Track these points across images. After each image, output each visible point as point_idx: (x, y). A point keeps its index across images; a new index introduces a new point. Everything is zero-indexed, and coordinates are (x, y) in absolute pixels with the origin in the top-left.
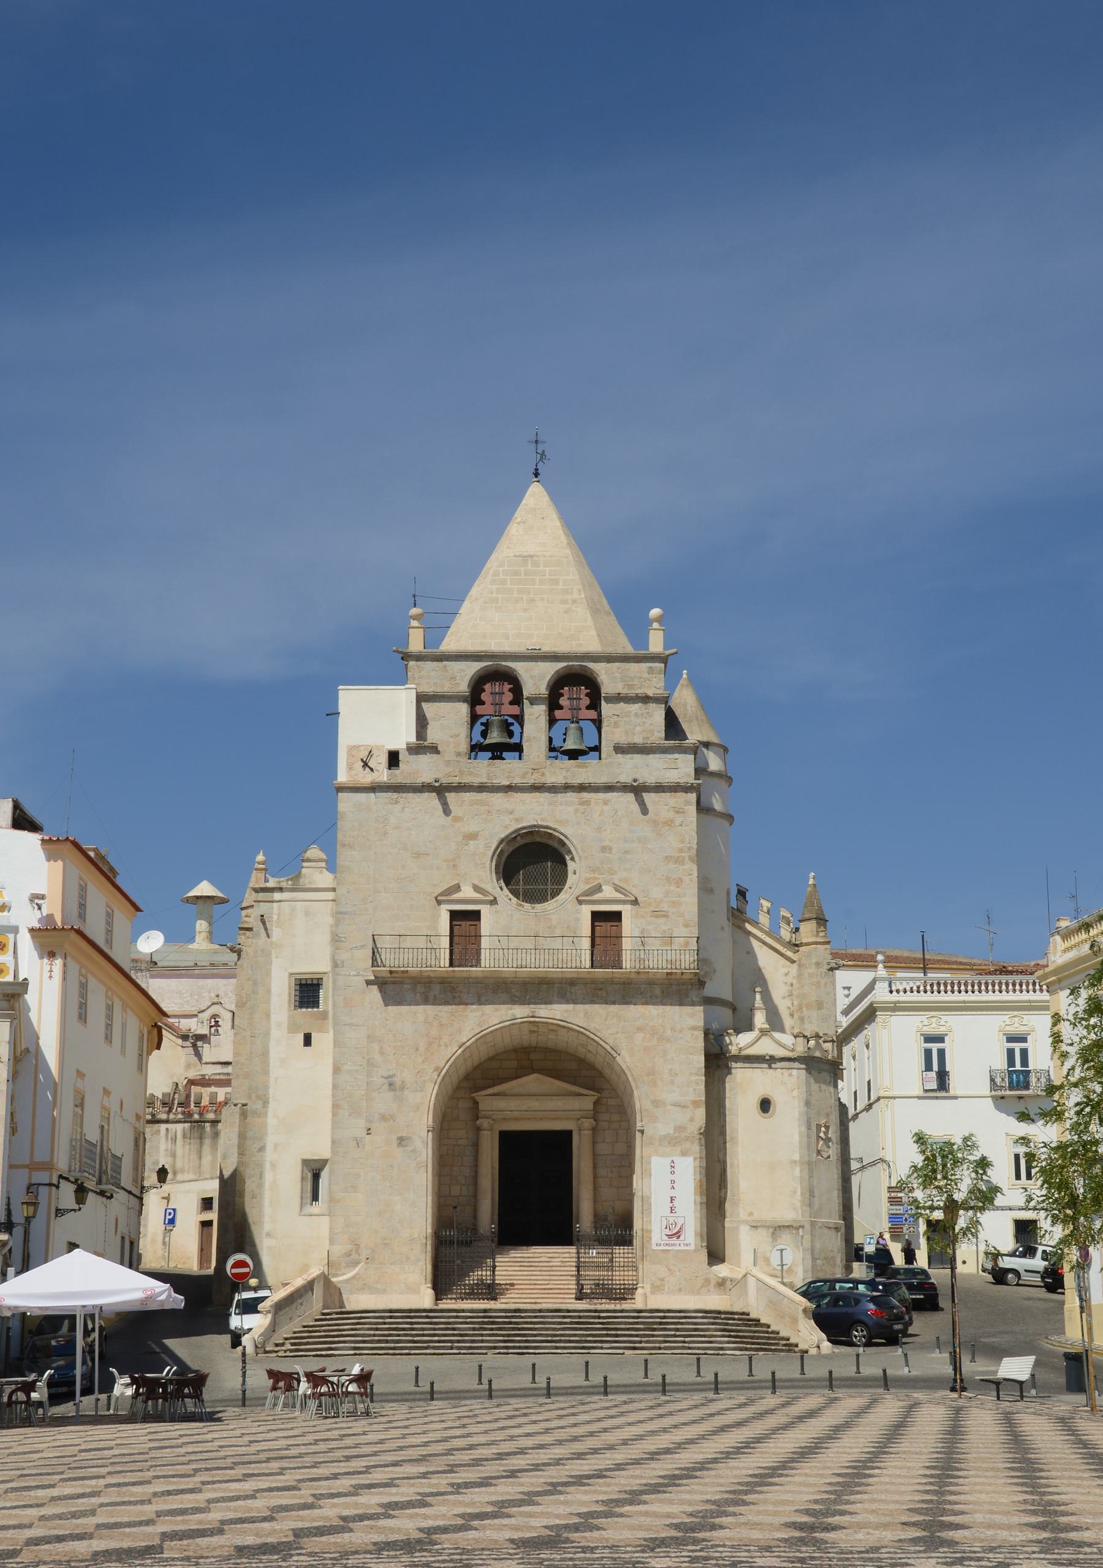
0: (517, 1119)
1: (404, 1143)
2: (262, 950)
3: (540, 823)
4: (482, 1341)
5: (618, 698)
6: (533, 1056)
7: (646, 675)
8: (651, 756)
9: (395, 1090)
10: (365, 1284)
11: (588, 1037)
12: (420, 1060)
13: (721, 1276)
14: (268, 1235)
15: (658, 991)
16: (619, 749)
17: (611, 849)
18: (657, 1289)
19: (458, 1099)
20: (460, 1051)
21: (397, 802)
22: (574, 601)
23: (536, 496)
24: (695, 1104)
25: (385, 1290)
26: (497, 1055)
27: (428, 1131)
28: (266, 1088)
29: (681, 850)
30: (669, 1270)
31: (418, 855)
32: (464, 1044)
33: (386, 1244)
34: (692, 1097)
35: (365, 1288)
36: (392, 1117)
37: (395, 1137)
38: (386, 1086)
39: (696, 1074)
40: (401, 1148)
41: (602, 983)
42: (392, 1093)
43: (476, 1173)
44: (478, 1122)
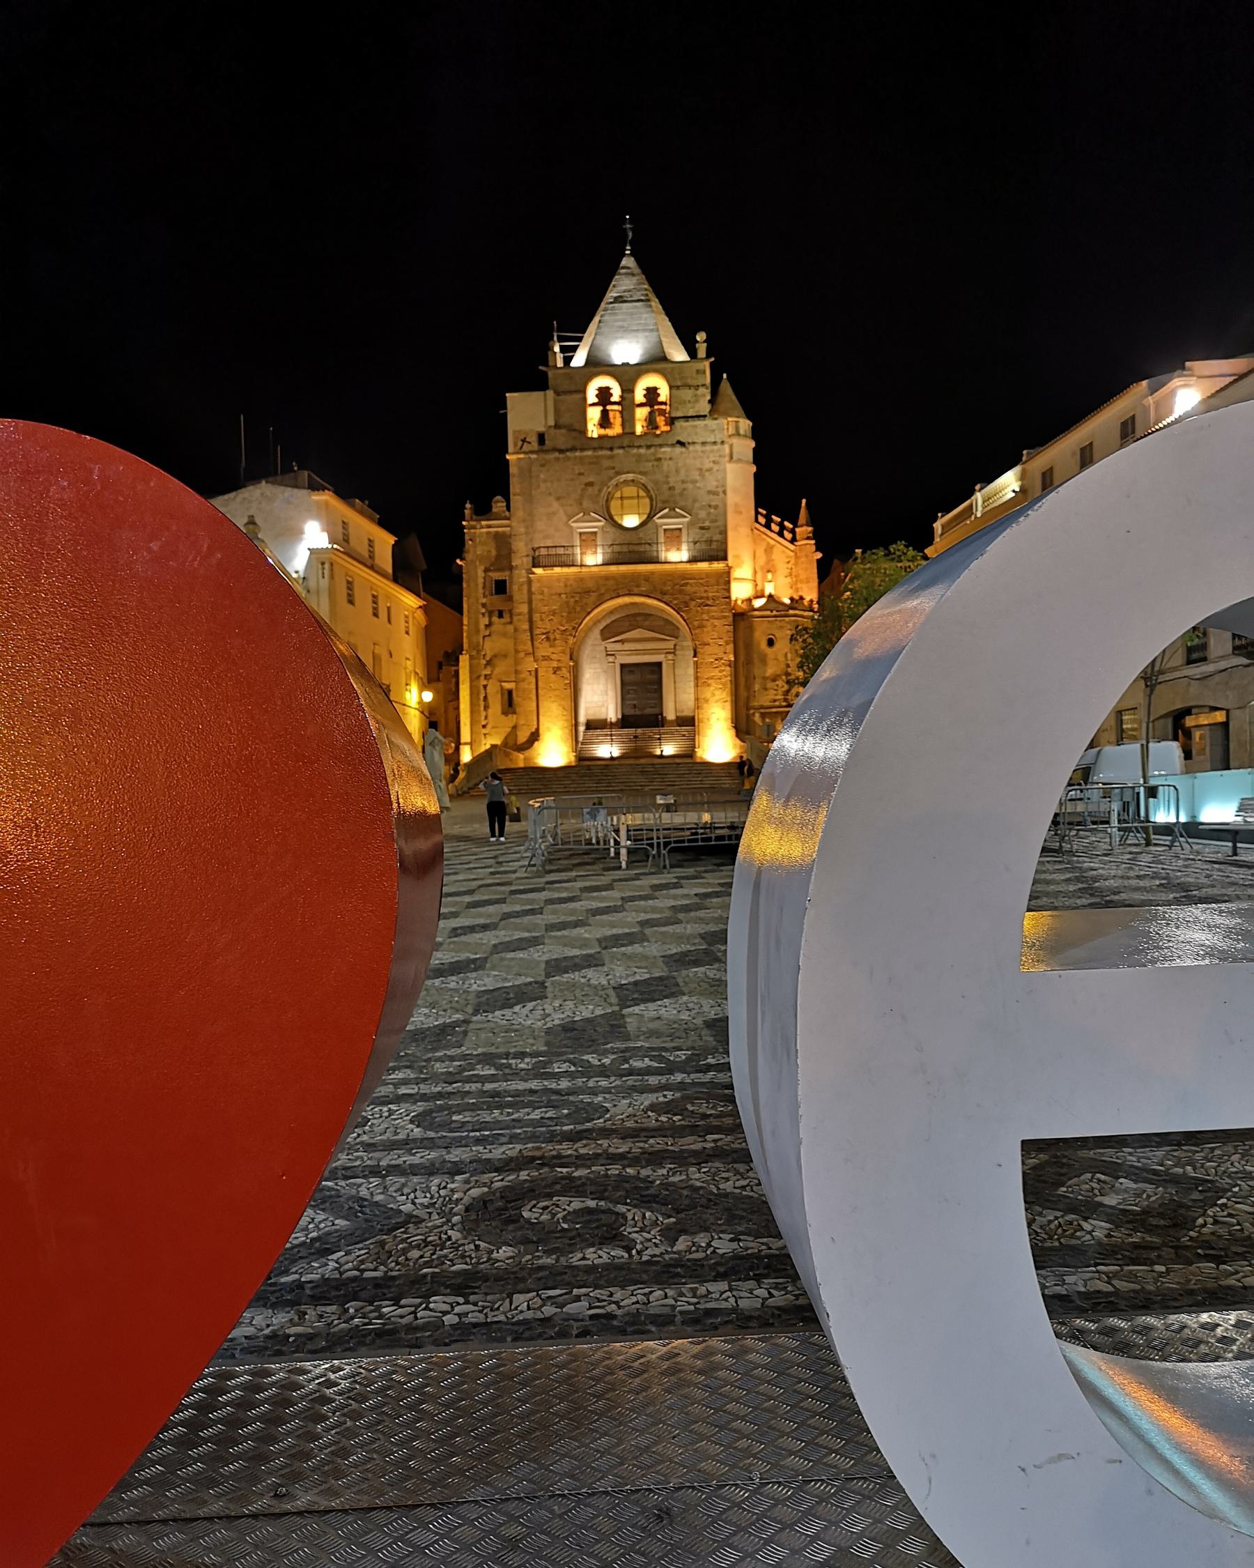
14: (484, 726)
28: (478, 643)
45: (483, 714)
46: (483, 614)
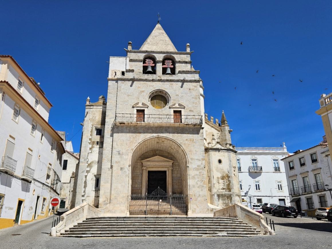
0: (152, 167)
1: (122, 169)
2: (87, 120)
3: (160, 89)
4: (145, 230)
5: (180, 62)
6: (157, 152)
7: (186, 57)
8: (188, 74)
9: (120, 155)
10: (109, 210)
11: (173, 141)
12: (127, 147)
13: (211, 208)
14: (83, 196)
15: (191, 130)
16: (180, 72)
17: (178, 95)
18: (193, 212)
19: (138, 162)
20: (138, 145)
21: (123, 83)
22: (168, 44)
23: (158, 26)
24: (203, 159)
25: (115, 212)
26: (148, 151)
27: (129, 166)
29: (196, 96)
30: (197, 206)
31: (128, 96)
32: (139, 143)
33: (116, 198)
34: (201, 157)
35: (109, 211)
36: (119, 162)
37: (119, 168)
38: (118, 154)
39: (202, 152)
40: (121, 171)
41: (177, 128)
42: (119, 156)
43: (142, 181)
44: (143, 168)
45: (84, 189)
46: (90, 143)
